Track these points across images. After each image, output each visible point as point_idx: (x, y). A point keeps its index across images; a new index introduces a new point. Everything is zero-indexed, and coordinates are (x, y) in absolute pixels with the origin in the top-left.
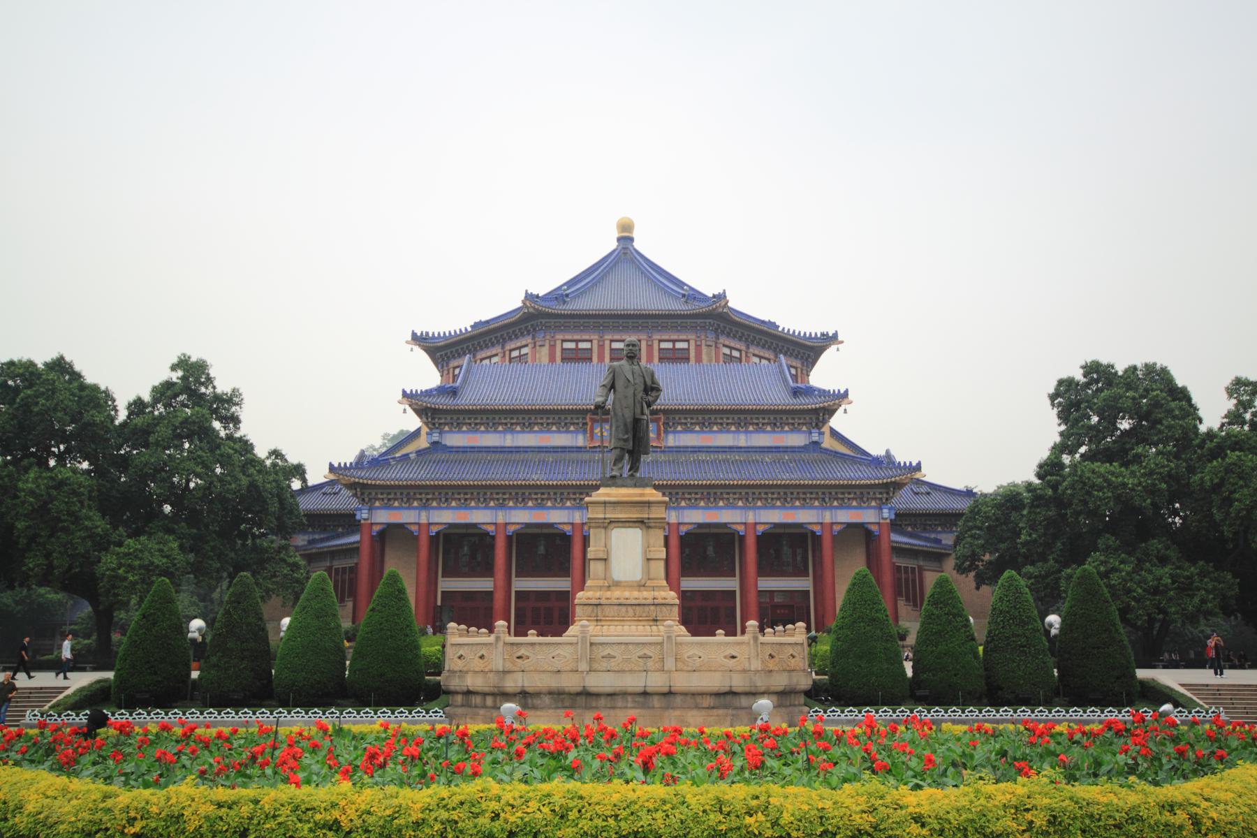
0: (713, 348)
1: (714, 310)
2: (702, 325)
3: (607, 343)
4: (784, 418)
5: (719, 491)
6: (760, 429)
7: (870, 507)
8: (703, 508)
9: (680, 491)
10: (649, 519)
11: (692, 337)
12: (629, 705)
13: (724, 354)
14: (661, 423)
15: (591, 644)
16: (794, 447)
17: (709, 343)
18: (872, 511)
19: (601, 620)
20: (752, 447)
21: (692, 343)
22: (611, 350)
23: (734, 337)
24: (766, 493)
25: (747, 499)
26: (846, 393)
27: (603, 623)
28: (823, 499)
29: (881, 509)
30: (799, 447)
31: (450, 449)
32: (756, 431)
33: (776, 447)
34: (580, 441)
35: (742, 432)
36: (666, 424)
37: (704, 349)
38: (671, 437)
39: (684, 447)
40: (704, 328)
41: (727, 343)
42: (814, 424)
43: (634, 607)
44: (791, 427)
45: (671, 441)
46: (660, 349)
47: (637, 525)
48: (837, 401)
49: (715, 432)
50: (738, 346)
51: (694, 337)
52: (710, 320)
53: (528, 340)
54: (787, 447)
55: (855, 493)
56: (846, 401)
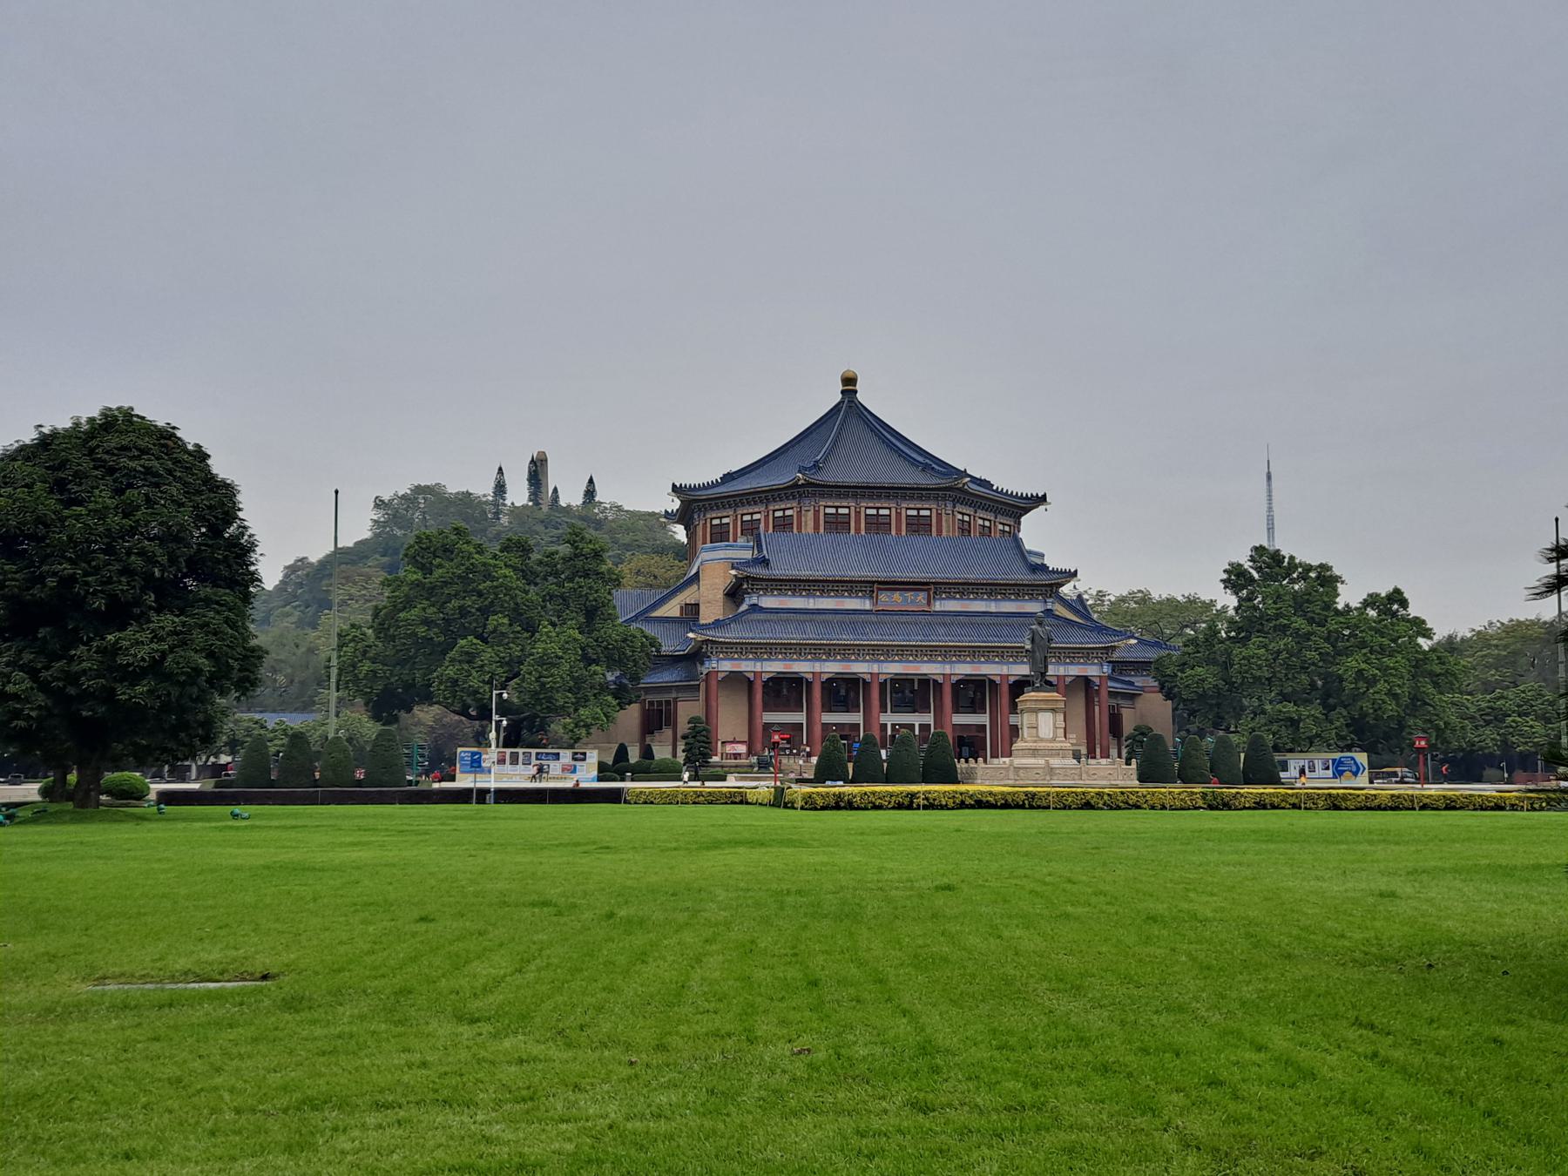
3: (863, 509)
5: (981, 650)
6: (1006, 598)
7: (1093, 664)
8: (969, 662)
18: (1094, 667)
21: (934, 511)
22: (866, 515)
26: (1076, 572)
28: (1059, 658)
31: (762, 610)
34: (867, 605)
36: (935, 593)
37: (944, 519)
38: (938, 603)
40: (944, 499)
45: (938, 606)
46: (907, 516)
50: (968, 512)
53: (795, 504)
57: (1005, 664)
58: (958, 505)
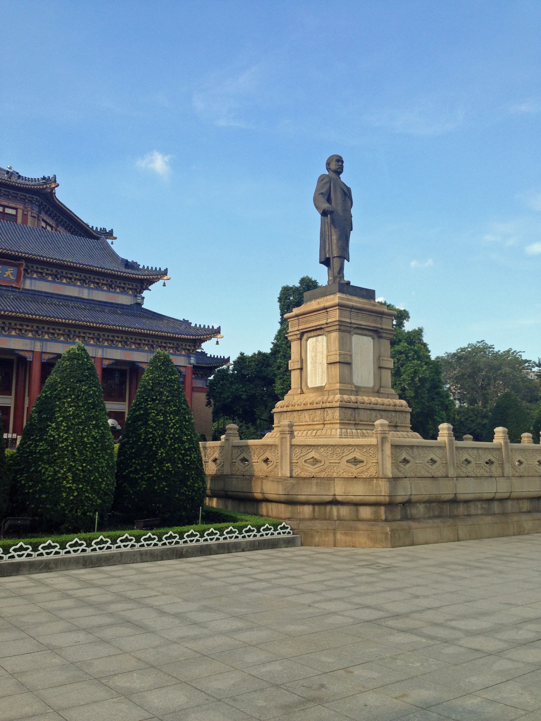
0: (36, 219)
1: (43, 189)
2: (30, 199)
4: (118, 282)
6: (98, 286)
9: (46, 327)
10: (382, 329)
11: (20, 206)
12: (480, 512)
13: (42, 226)
14: (22, 269)
15: (457, 448)
16: (123, 305)
17: (34, 215)
18: (182, 358)
19: (358, 424)
20: (93, 300)
21: (20, 212)
23: (50, 215)
24: (113, 336)
25: (98, 339)
26: (165, 273)
27: (360, 427)
28: (152, 346)
29: (189, 357)
30: (126, 306)
32: (96, 289)
35: (86, 288)
36: (26, 270)
37: (30, 219)
39: (38, 291)
41: (45, 218)
42: (138, 290)
43: (381, 412)
44: (121, 290)
45: (28, 285)
47: (371, 333)
48: (159, 276)
49: (64, 284)
50: (51, 223)
51: (22, 207)
52: (37, 197)
54: (118, 304)
55: (173, 344)
56: (165, 278)
57: (100, 347)
58: (43, 213)
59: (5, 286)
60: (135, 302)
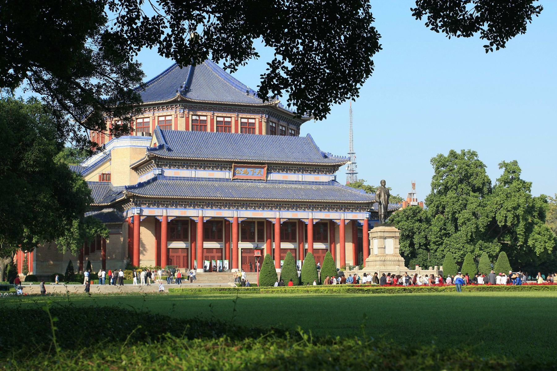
1: (271, 104)
33: (316, 182)
40: (263, 113)
50: (275, 121)
59: (258, 180)
60: (331, 179)
